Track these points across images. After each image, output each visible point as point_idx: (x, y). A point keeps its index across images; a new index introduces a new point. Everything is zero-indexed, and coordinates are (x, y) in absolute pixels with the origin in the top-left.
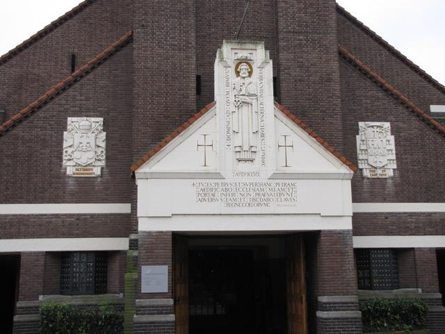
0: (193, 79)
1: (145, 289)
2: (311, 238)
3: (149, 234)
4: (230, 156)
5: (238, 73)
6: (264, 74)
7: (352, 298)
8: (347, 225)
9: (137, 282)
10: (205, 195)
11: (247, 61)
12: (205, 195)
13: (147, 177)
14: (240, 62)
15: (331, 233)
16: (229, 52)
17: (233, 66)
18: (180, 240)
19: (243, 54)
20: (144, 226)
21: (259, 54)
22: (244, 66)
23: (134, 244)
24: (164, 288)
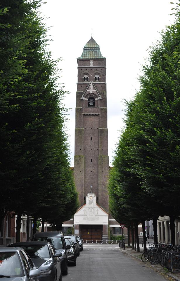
0: (84, 197)
1: (75, 233)
2: (102, 225)
3: (76, 225)
4: (89, 213)
5: (90, 198)
6: (94, 199)
7: (107, 235)
8: (107, 224)
9: (74, 232)
10: (84, 219)
11: (91, 196)
12: (84, 219)
13: (76, 216)
14: (91, 196)
15: (104, 225)
16: (89, 195)
17: (89, 197)
18: (80, 225)
19: (91, 195)
20: (75, 223)
21: (93, 195)
22: (91, 197)
23: (74, 226)
24: (78, 233)
